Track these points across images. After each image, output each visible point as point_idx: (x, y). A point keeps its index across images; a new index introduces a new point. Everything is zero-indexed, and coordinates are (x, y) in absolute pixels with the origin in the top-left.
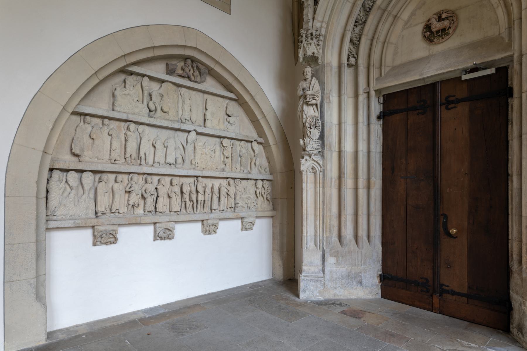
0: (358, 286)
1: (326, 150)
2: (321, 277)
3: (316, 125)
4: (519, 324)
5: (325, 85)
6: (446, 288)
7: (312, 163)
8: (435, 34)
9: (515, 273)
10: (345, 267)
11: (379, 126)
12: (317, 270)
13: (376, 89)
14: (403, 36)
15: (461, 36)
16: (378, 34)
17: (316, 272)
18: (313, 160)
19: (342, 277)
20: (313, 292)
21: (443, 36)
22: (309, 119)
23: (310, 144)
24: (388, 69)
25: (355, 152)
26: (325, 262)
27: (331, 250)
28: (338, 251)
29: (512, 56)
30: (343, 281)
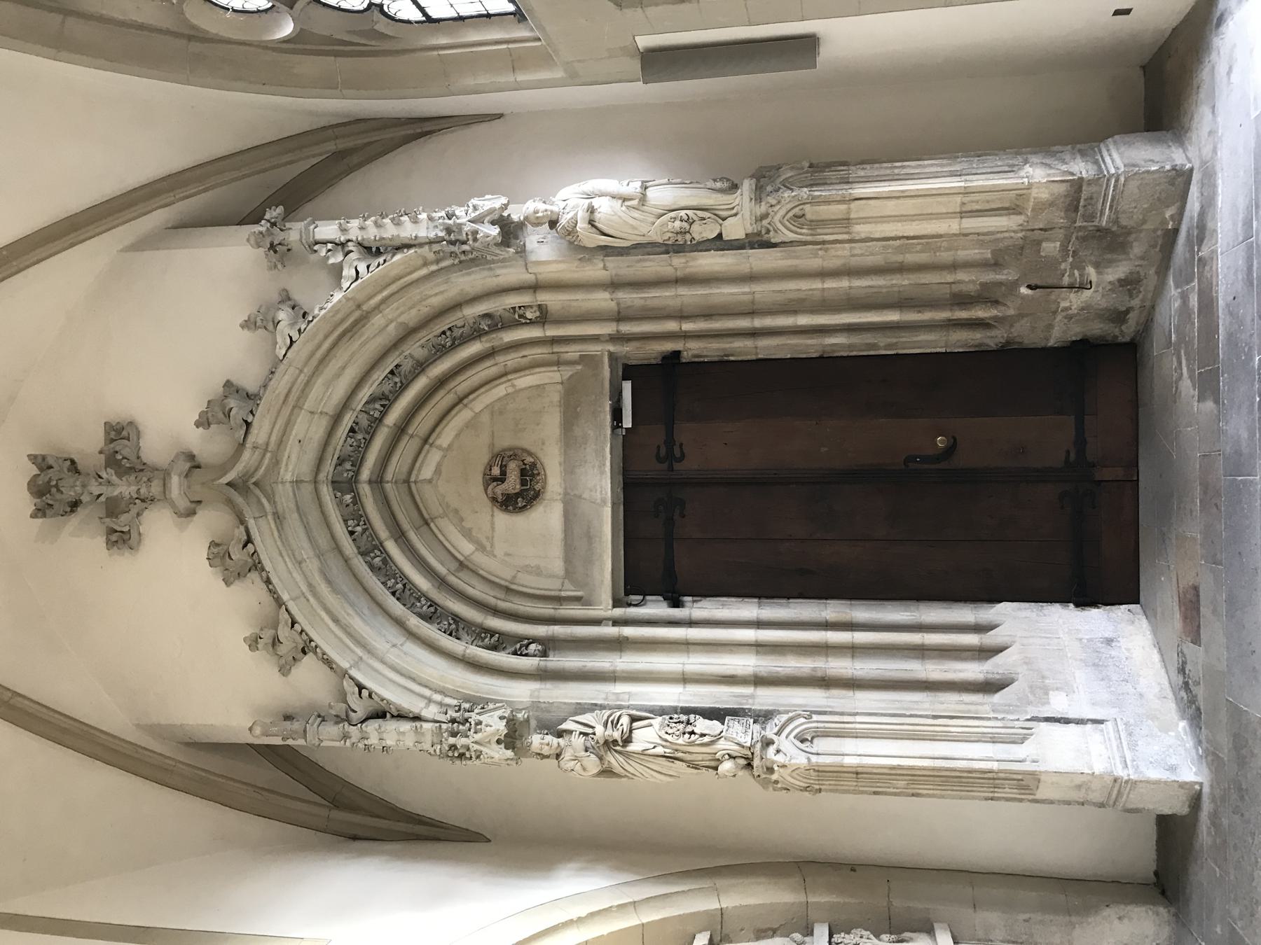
0: (1120, 647)
1: (753, 704)
2: (1117, 724)
3: (685, 722)
4: (1109, 320)
5: (584, 702)
6: (1073, 456)
7: (787, 737)
8: (525, 487)
9: (1011, 333)
10: (1074, 673)
11: (695, 605)
12: (1097, 737)
13: (611, 602)
14: (507, 554)
15: (543, 444)
16: (487, 597)
17: (1104, 739)
18: (778, 733)
19: (1103, 680)
20: (1170, 747)
21: (535, 472)
22: (669, 738)
23: (734, 736)
24: (568, 585)
25: (758, 653)
26: (1066, 716)
27: (1030, 703)
28: (1031, 687)
29: (611, 354)
30: (1115, 677)
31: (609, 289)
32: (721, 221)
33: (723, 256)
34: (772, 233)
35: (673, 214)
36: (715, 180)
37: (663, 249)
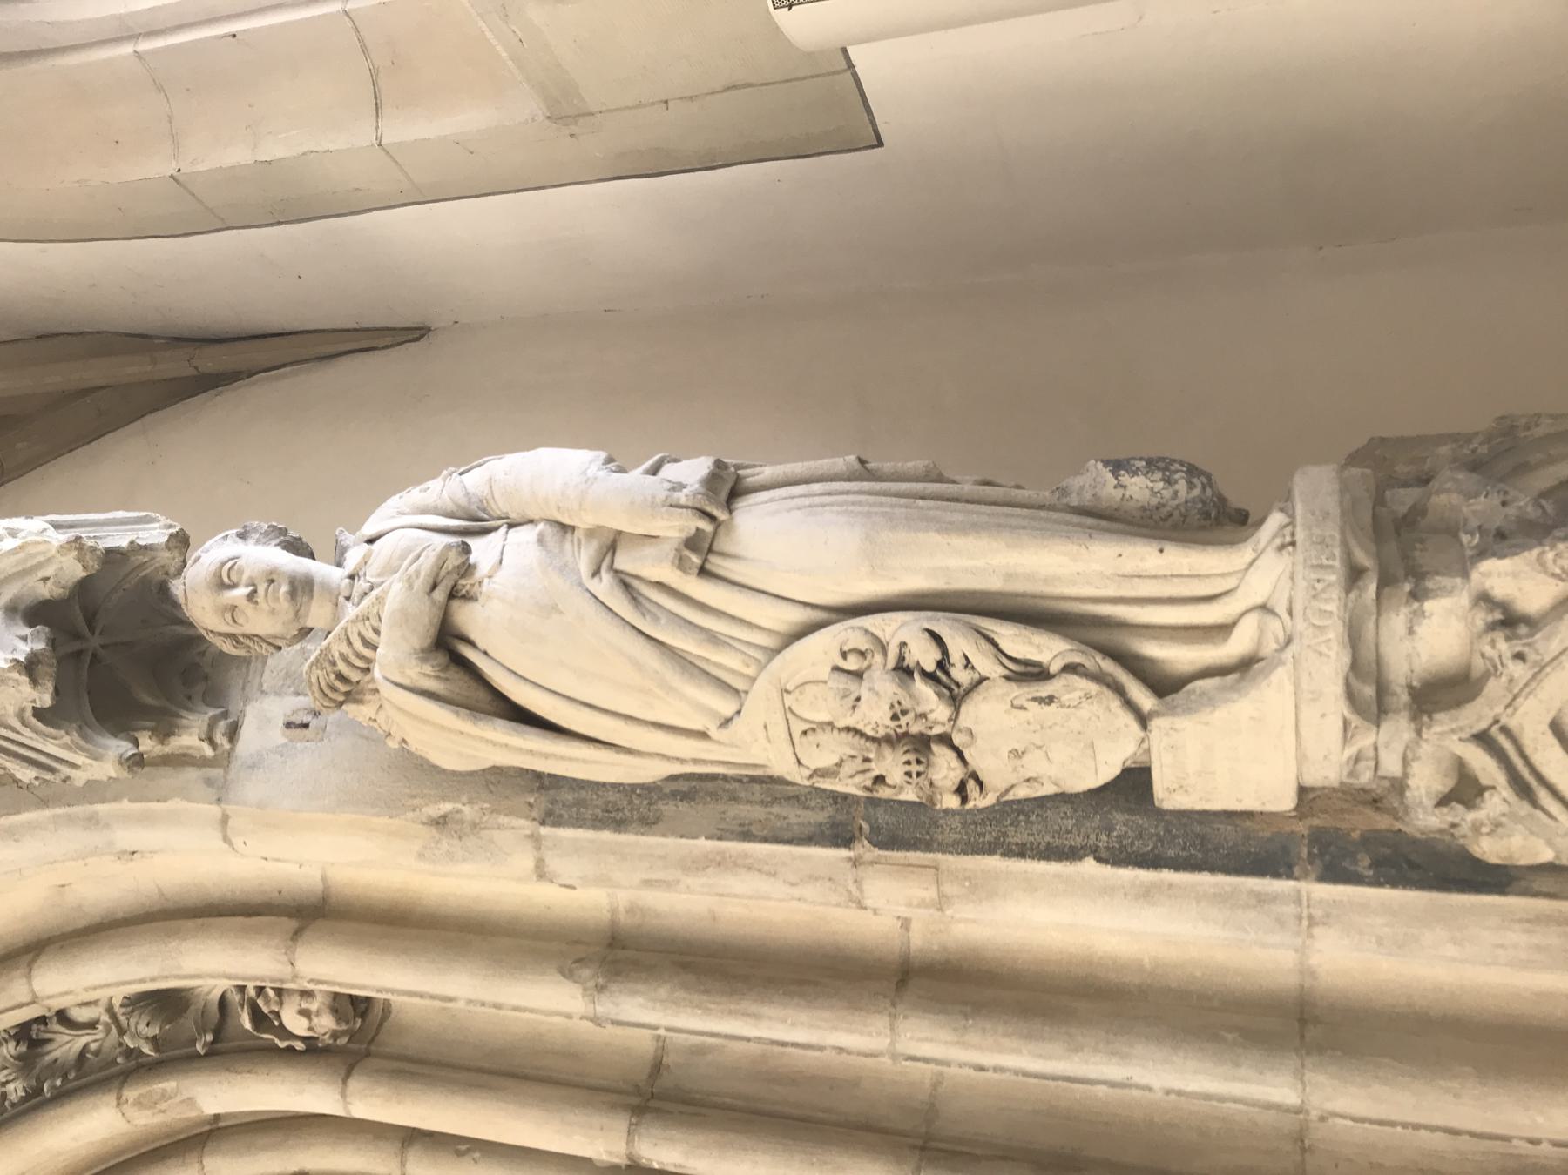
31: (586, 973)
32: (1146, 701)
33: (1146, 894)
34: (1499, 801)
35: (848, 633)
36: (1117, 466)
37: (818, 817)
